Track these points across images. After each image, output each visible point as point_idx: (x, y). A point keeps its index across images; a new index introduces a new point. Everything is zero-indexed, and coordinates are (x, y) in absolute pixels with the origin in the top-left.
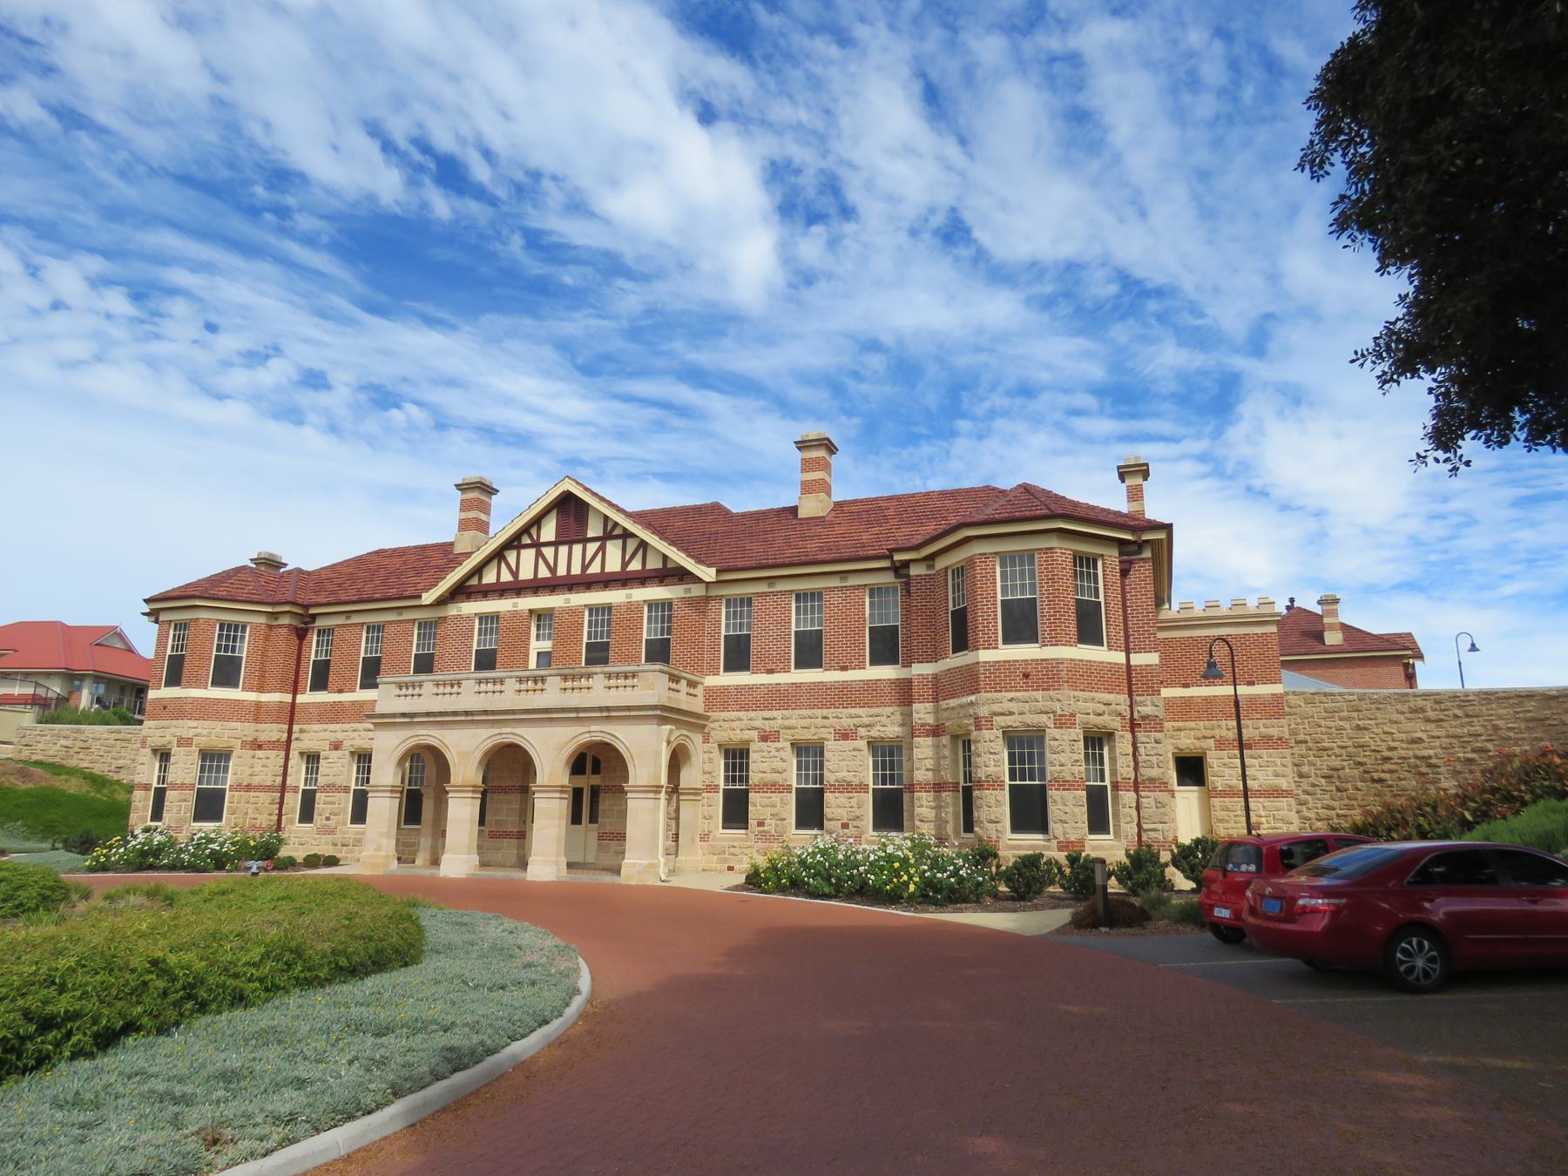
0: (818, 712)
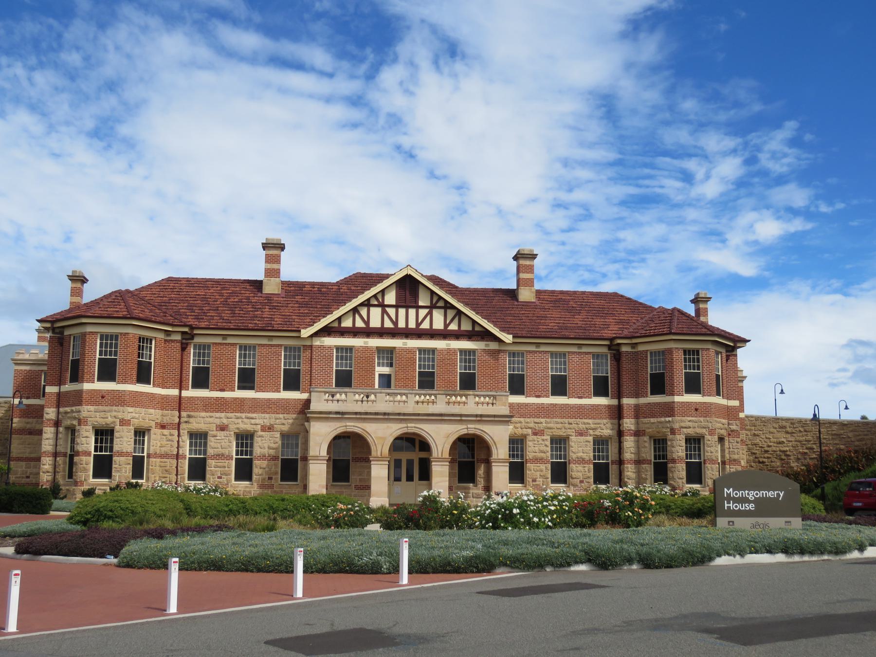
0: (566, 421)
